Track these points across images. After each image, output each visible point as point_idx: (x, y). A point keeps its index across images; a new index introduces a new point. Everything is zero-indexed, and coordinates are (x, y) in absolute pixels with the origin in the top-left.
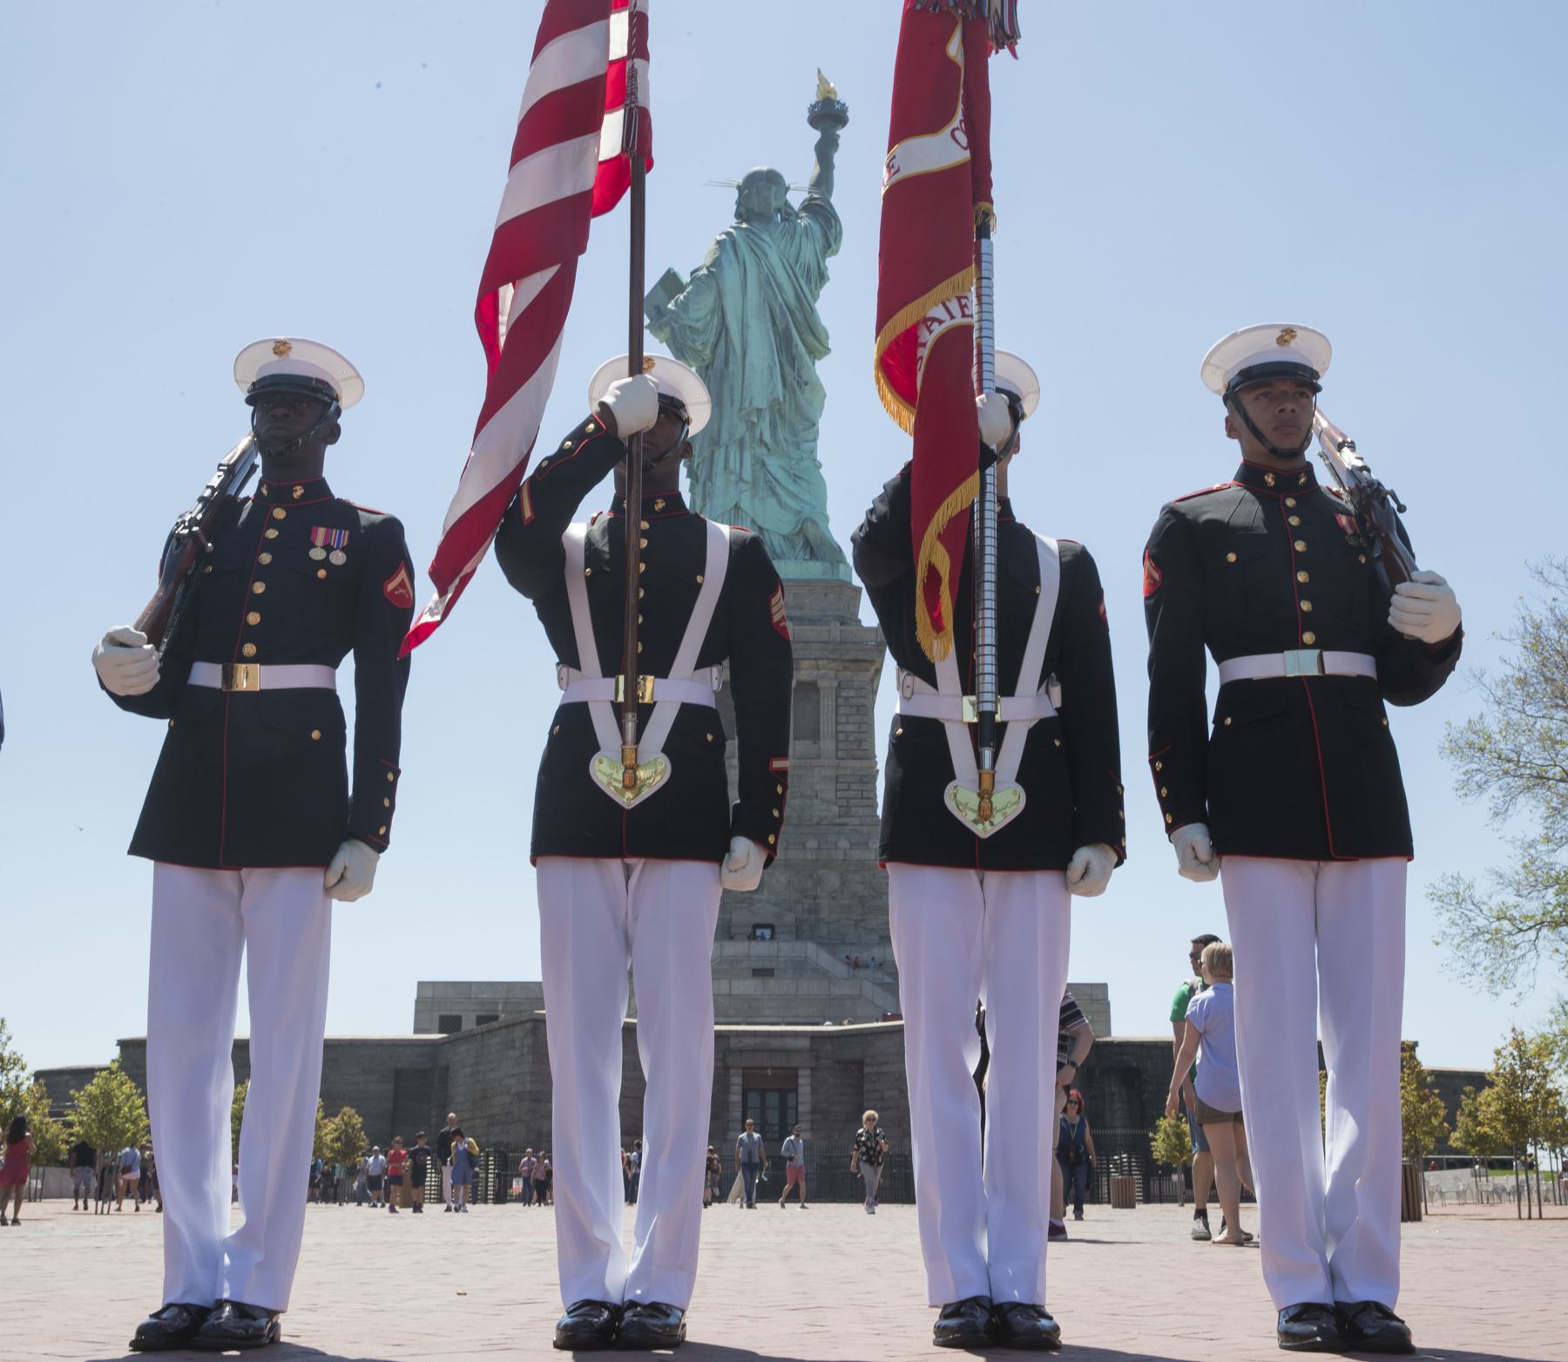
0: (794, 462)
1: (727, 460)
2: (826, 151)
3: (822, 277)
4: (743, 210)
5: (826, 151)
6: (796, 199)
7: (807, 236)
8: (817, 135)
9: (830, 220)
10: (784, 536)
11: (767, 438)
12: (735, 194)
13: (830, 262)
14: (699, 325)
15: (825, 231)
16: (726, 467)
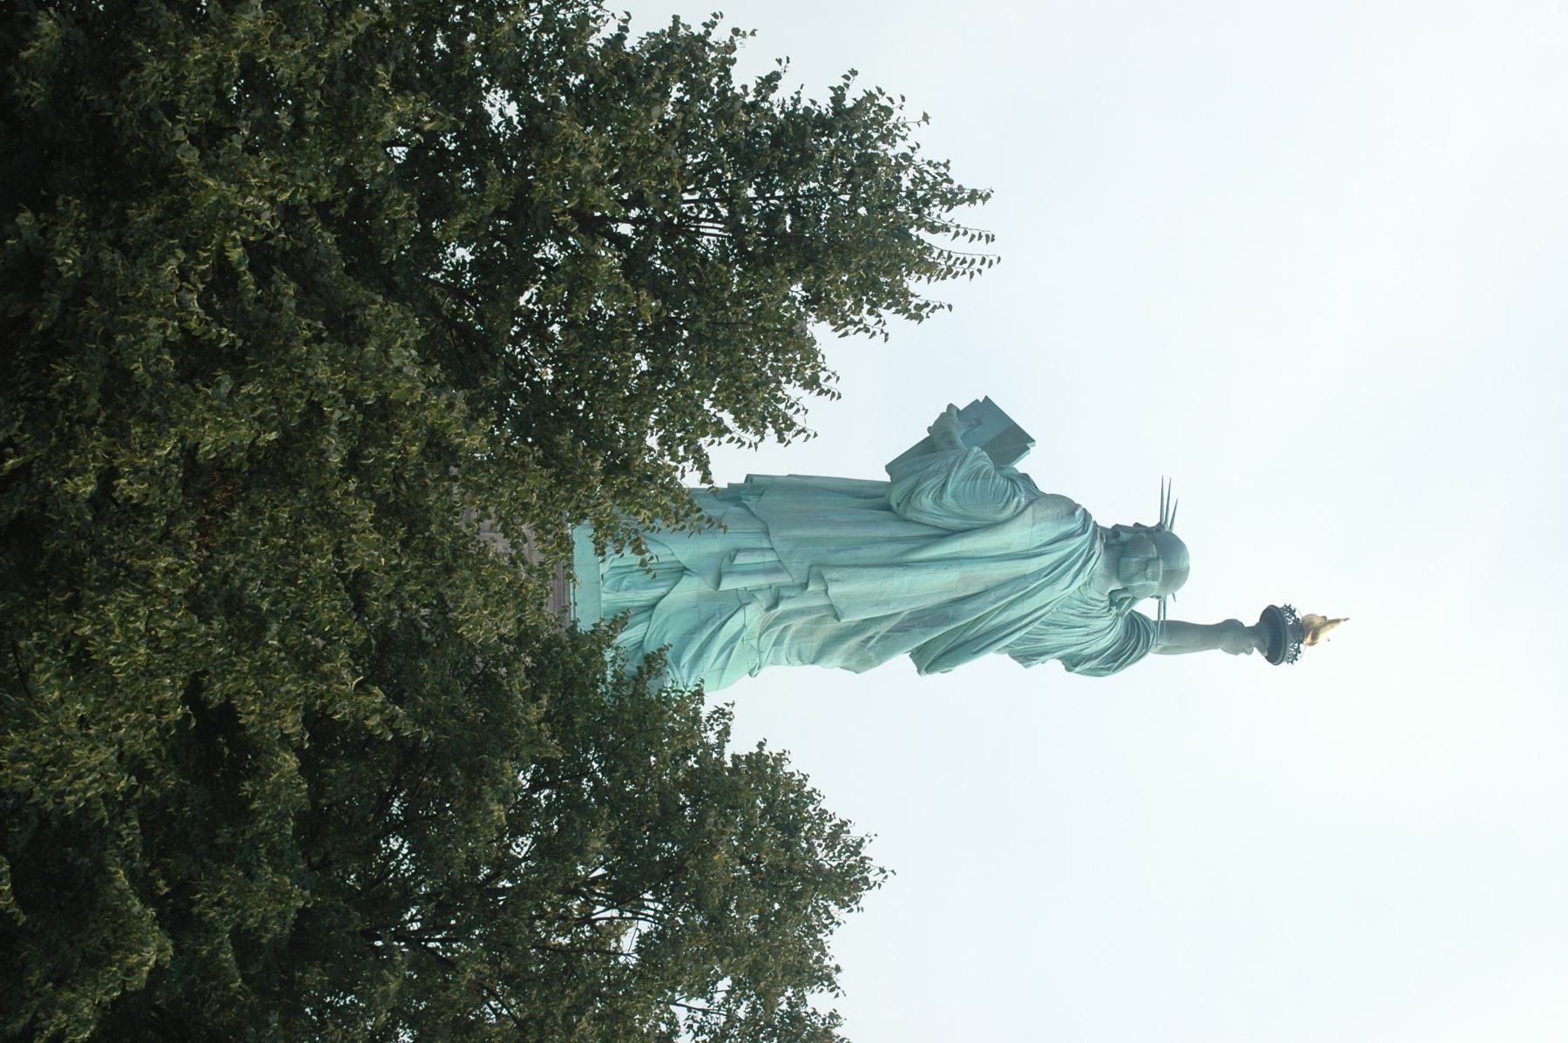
0: (754, 642)
1: (751, 550)
2: (1227, 634)
3: (1026, 657)
4: (1124, 536)
5: (1227, 634)
6: (1147, 608)
7: (1088, 634)
8: (1251, 619)
9: (1115, 661)
10: (642, 642)
11: (783, 607)
12: (1151, 521)
13: (1054, 666)
14: (948, 499)
15: (1096, 657)
16: (738, 551)
